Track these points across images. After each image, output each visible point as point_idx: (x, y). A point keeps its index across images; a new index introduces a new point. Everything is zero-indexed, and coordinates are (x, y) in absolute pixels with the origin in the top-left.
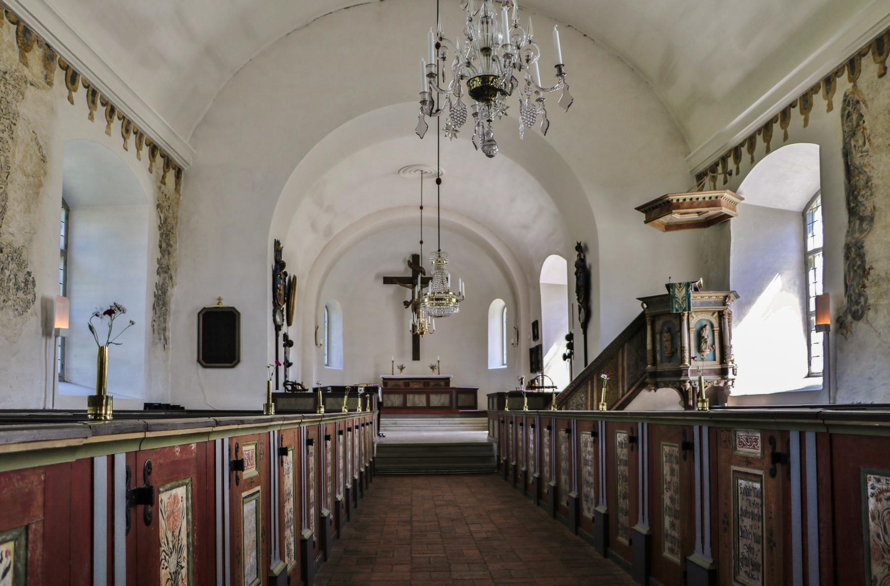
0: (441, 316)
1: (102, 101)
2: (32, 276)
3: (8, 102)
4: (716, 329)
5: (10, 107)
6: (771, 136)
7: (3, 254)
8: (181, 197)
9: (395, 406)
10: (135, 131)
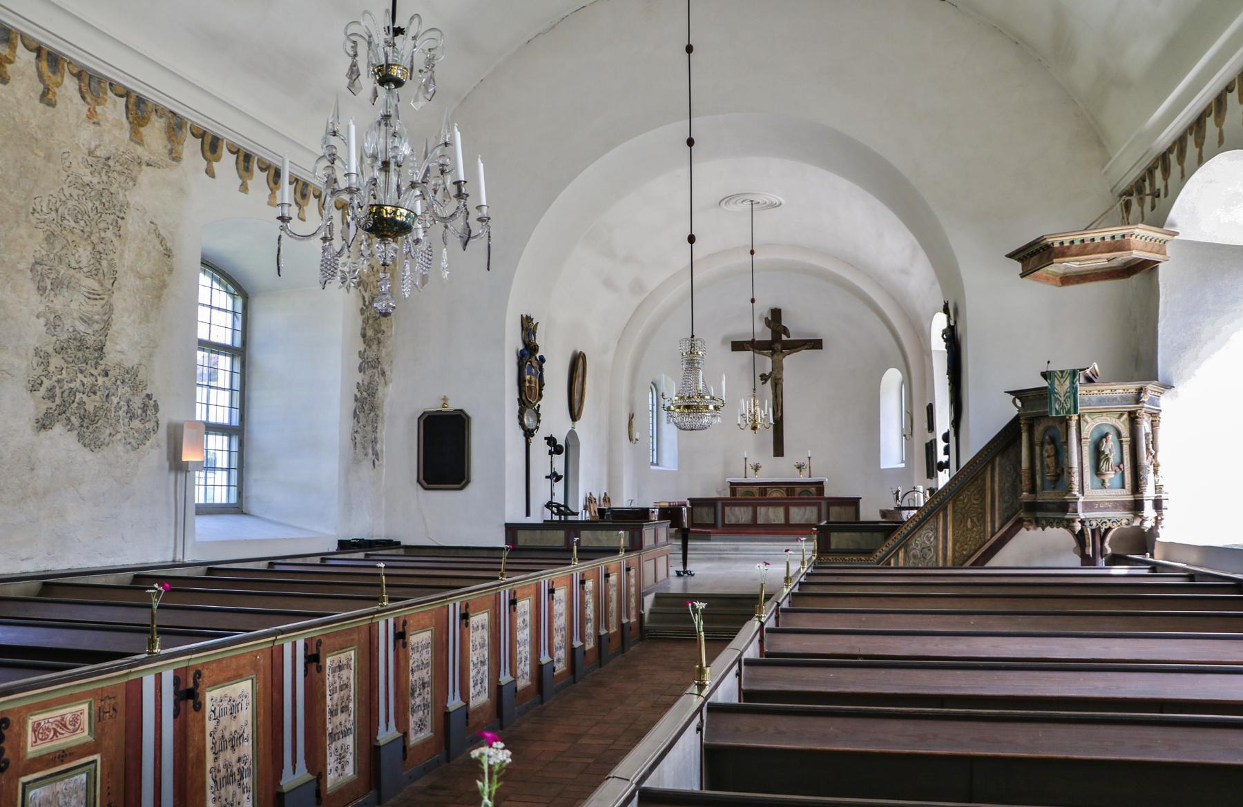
0: (692, 430)
1: (261, 166)
2: (153, 399)
3: (112, 194)
4: (1126, 437)
5: (115, 198)
6: (1204, 138)
7: (108, 378)
8: (398, 267)
10: (317, 194)
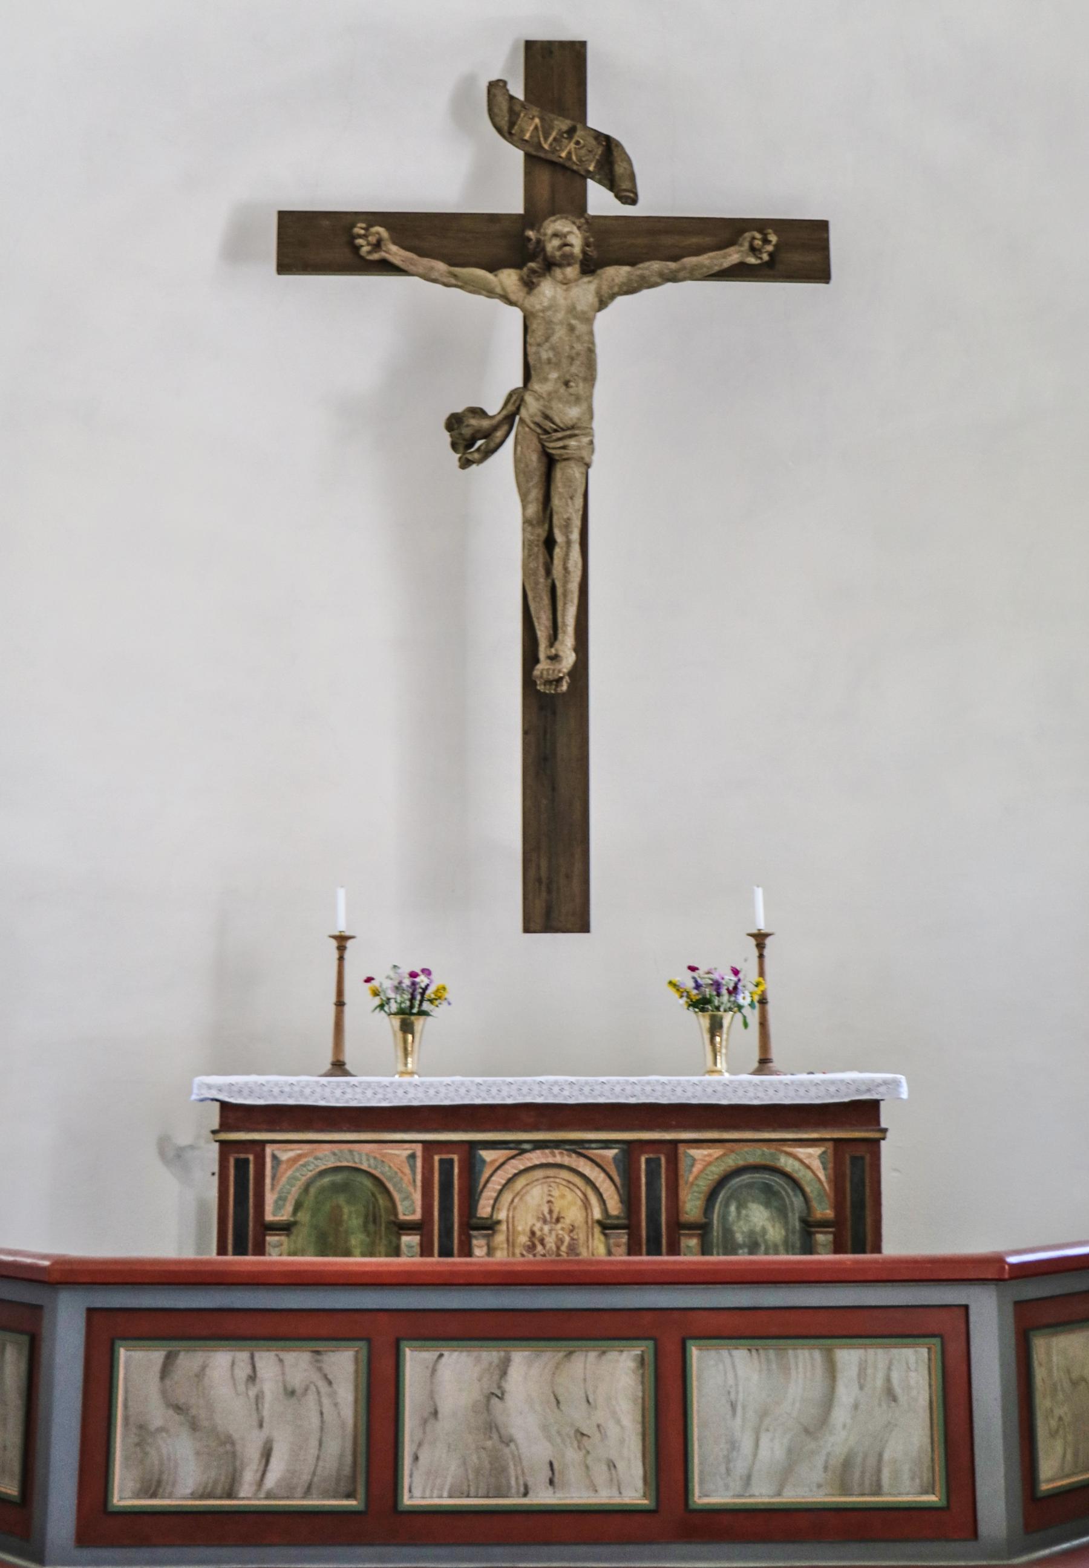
9: (247, 1496)
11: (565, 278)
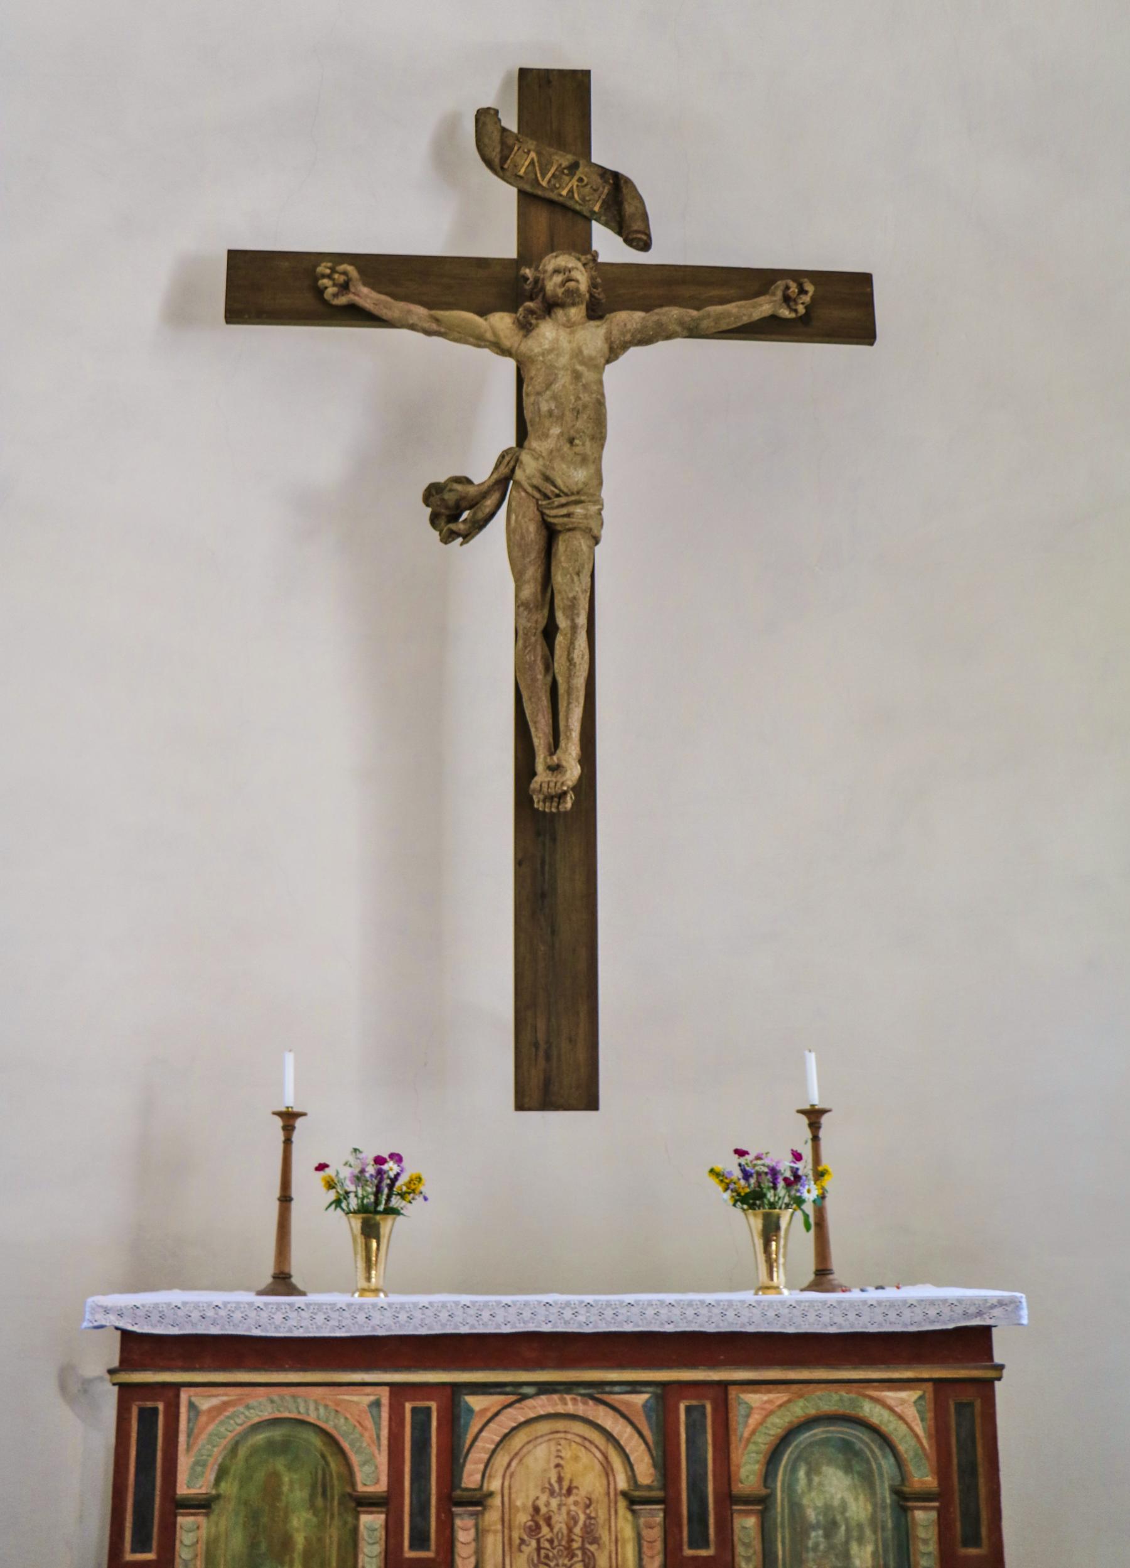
11: (569, 320)
